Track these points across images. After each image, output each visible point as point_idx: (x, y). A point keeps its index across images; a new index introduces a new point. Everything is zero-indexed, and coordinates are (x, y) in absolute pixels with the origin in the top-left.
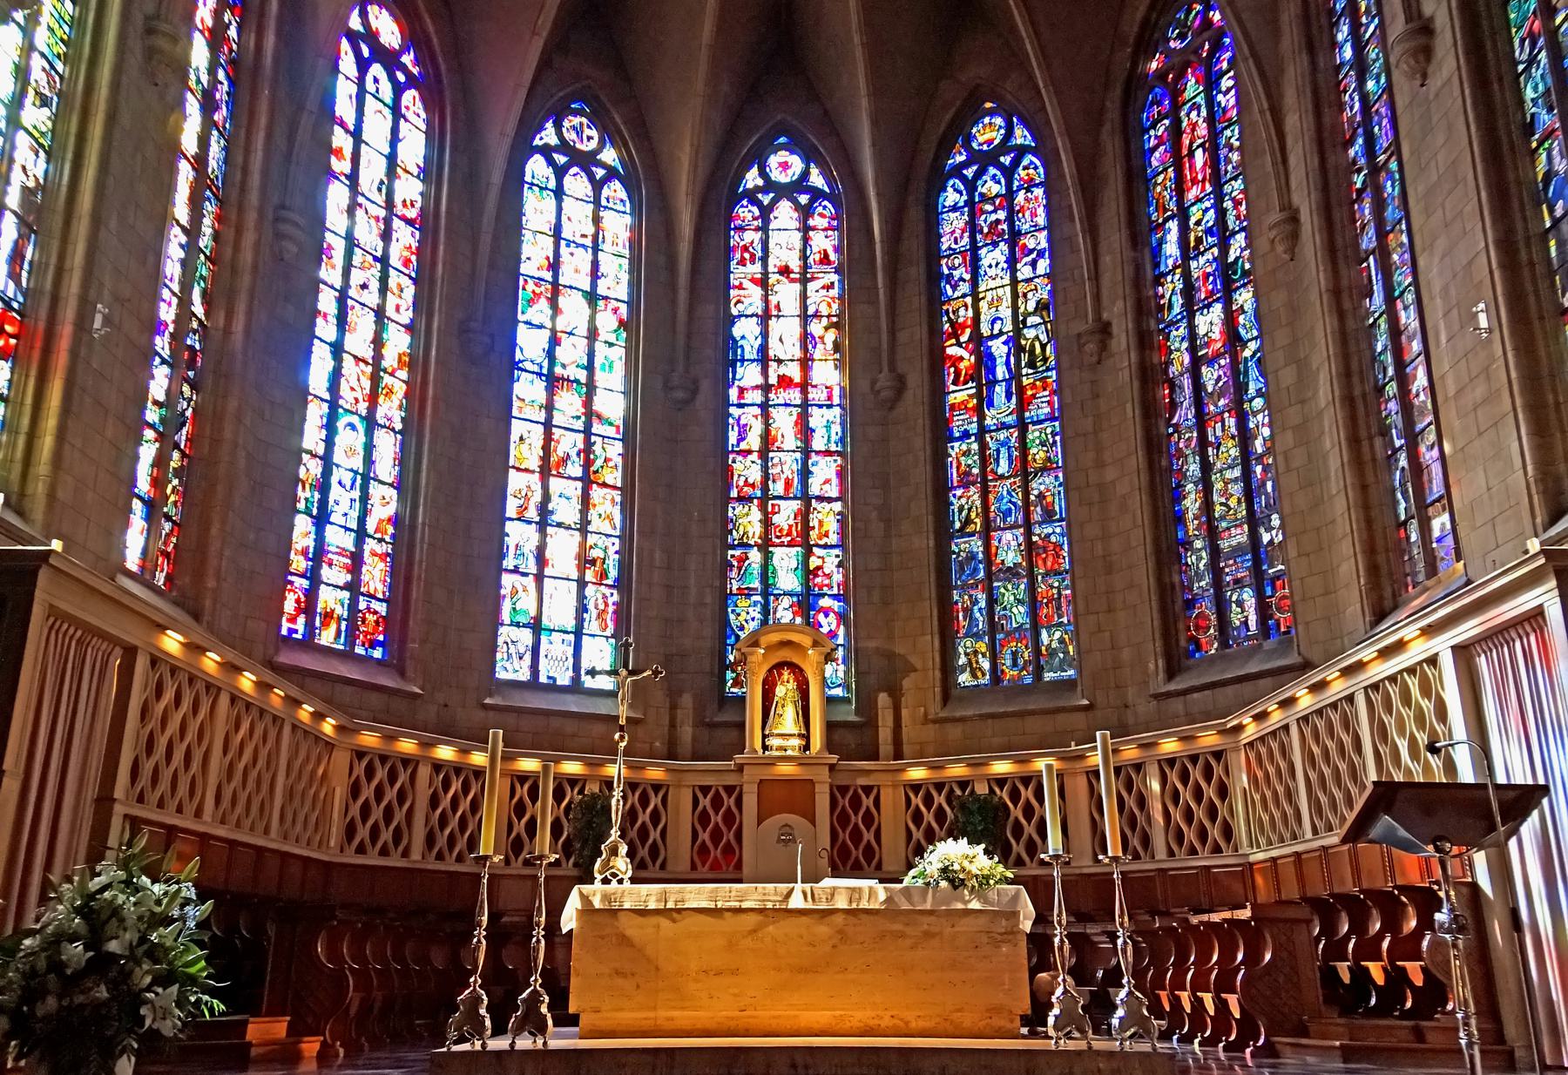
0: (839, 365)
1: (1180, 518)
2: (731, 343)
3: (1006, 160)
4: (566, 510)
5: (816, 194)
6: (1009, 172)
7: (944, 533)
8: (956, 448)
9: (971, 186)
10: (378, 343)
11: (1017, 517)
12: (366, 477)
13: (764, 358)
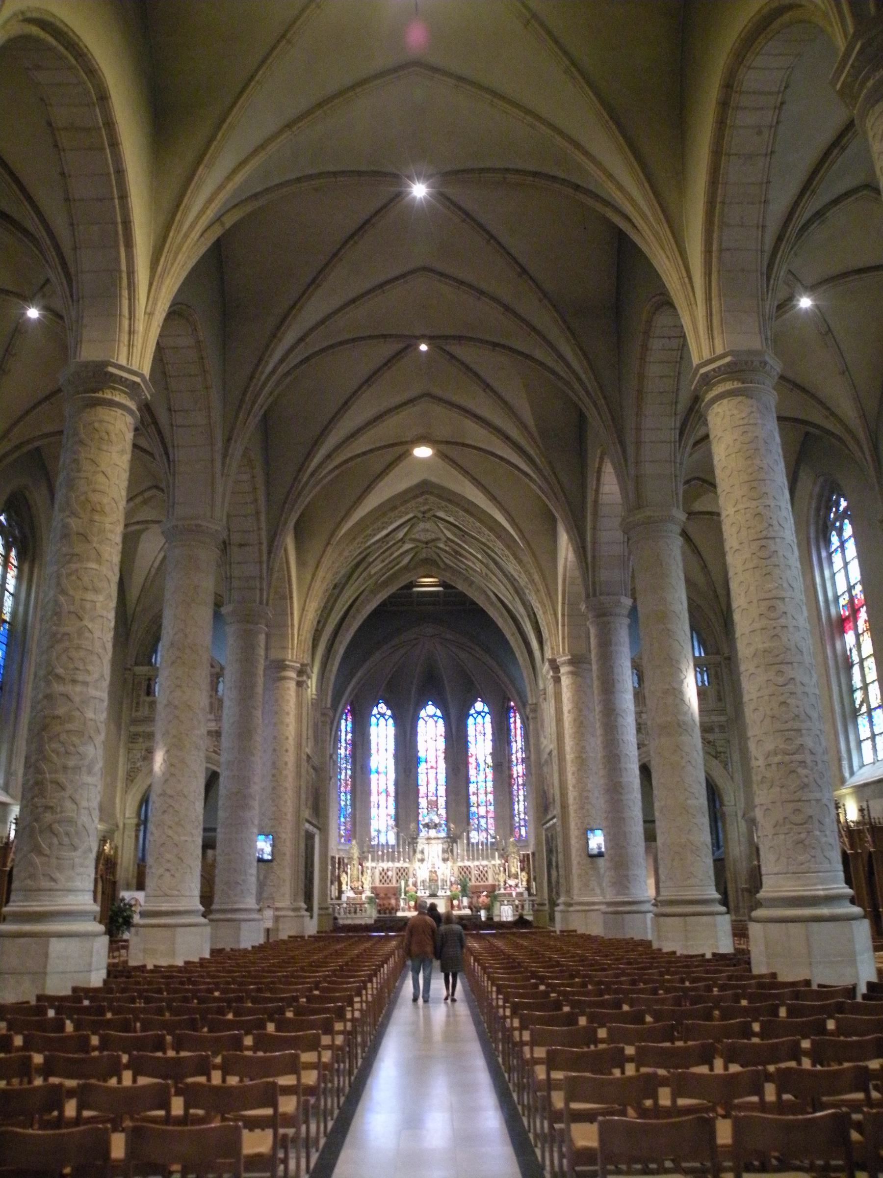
0: (446, 762)
1: (514, 810)
2: (418, 758)
3: (483, 714)
4: (383, 804)
5: (439, 717)
6: (483, 717)
7: (468, 805)
8: (471, 785)
9: (475, 719)
10: (346, 773)
11: (484, 804)
12: (346, 805)
13: (426, 762)
